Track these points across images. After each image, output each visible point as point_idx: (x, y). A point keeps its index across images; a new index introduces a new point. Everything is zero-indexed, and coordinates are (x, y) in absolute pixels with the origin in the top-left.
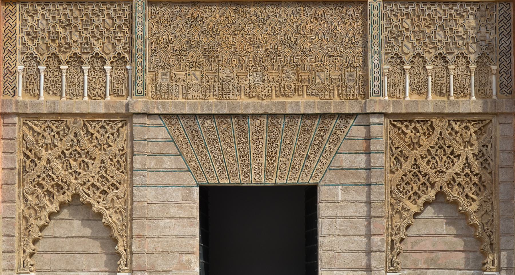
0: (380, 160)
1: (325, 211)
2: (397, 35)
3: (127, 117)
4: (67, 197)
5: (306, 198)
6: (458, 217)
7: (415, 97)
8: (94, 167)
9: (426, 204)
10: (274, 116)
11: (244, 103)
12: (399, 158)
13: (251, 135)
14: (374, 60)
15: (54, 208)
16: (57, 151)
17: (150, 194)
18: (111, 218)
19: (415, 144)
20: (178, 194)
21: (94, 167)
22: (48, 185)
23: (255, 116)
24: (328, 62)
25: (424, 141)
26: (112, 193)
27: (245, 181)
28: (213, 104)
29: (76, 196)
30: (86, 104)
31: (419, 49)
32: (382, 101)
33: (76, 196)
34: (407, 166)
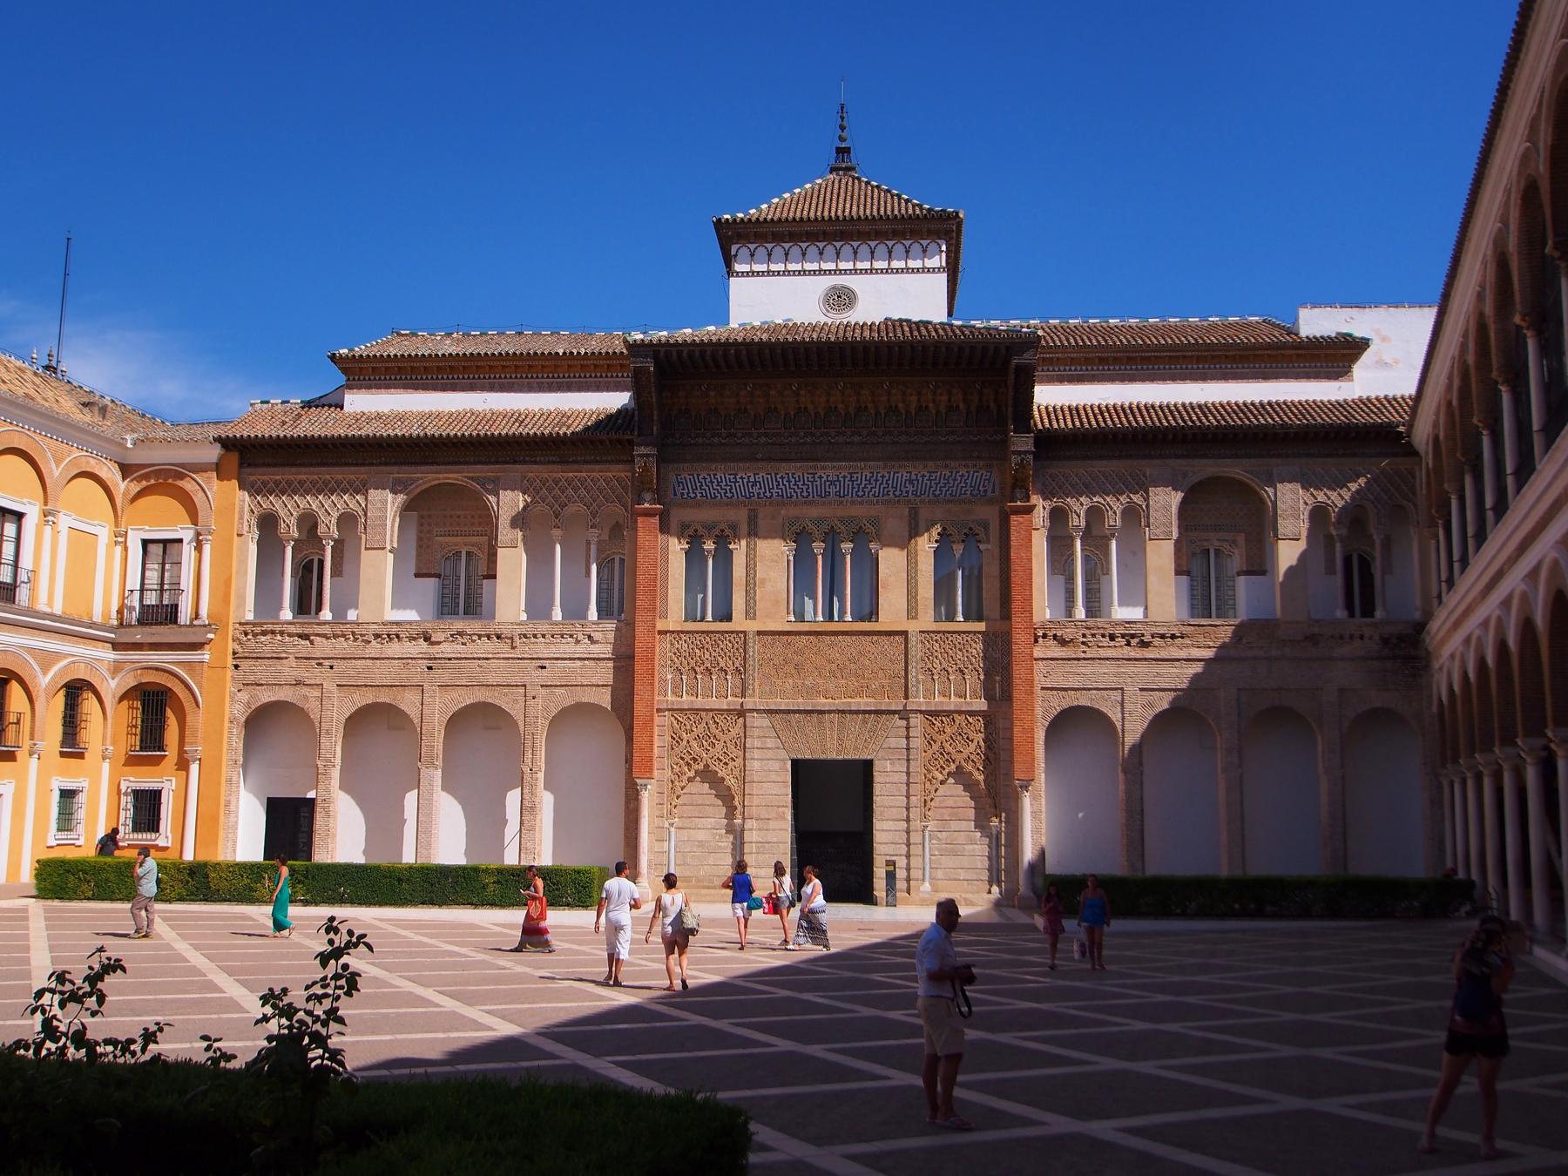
0: (917, 743)
1: (878, 777)
2: (929, 655)
3: (742, 713)
4: (701, 767)
5: (868, 765)
6: (970, 786)
7: (942, 699)
8: (719, 746)
9: (949, 774)
10: (843, 712)
11: (822, 703)
12: (931, 741)
13: (827, 725)
14: (912, 672)
15: (692, 774)
16: (694, 735)
17: (756, 765)
18: (730, 781)
19: (942, 732)
20: (776, 765)
21: (719, 746)
22: (687, 758)
23: (830, 712)
24: (881, 674)
25: (948, 730)
26: (731, 764)
27: (823, 757)
28: (801, 703)
29: (707, 766)
30: (714, 703)
31: (945, 665)
32: (919, 701)
33: (707, 766)
34: (936, 747)
